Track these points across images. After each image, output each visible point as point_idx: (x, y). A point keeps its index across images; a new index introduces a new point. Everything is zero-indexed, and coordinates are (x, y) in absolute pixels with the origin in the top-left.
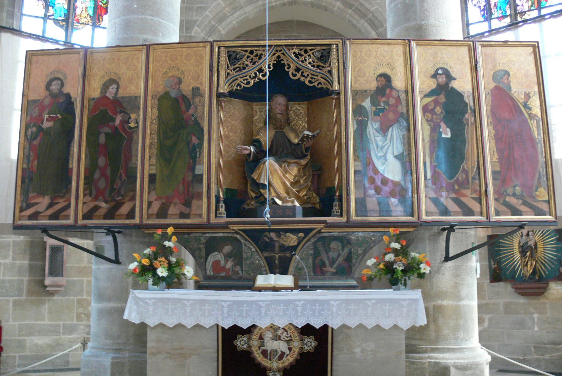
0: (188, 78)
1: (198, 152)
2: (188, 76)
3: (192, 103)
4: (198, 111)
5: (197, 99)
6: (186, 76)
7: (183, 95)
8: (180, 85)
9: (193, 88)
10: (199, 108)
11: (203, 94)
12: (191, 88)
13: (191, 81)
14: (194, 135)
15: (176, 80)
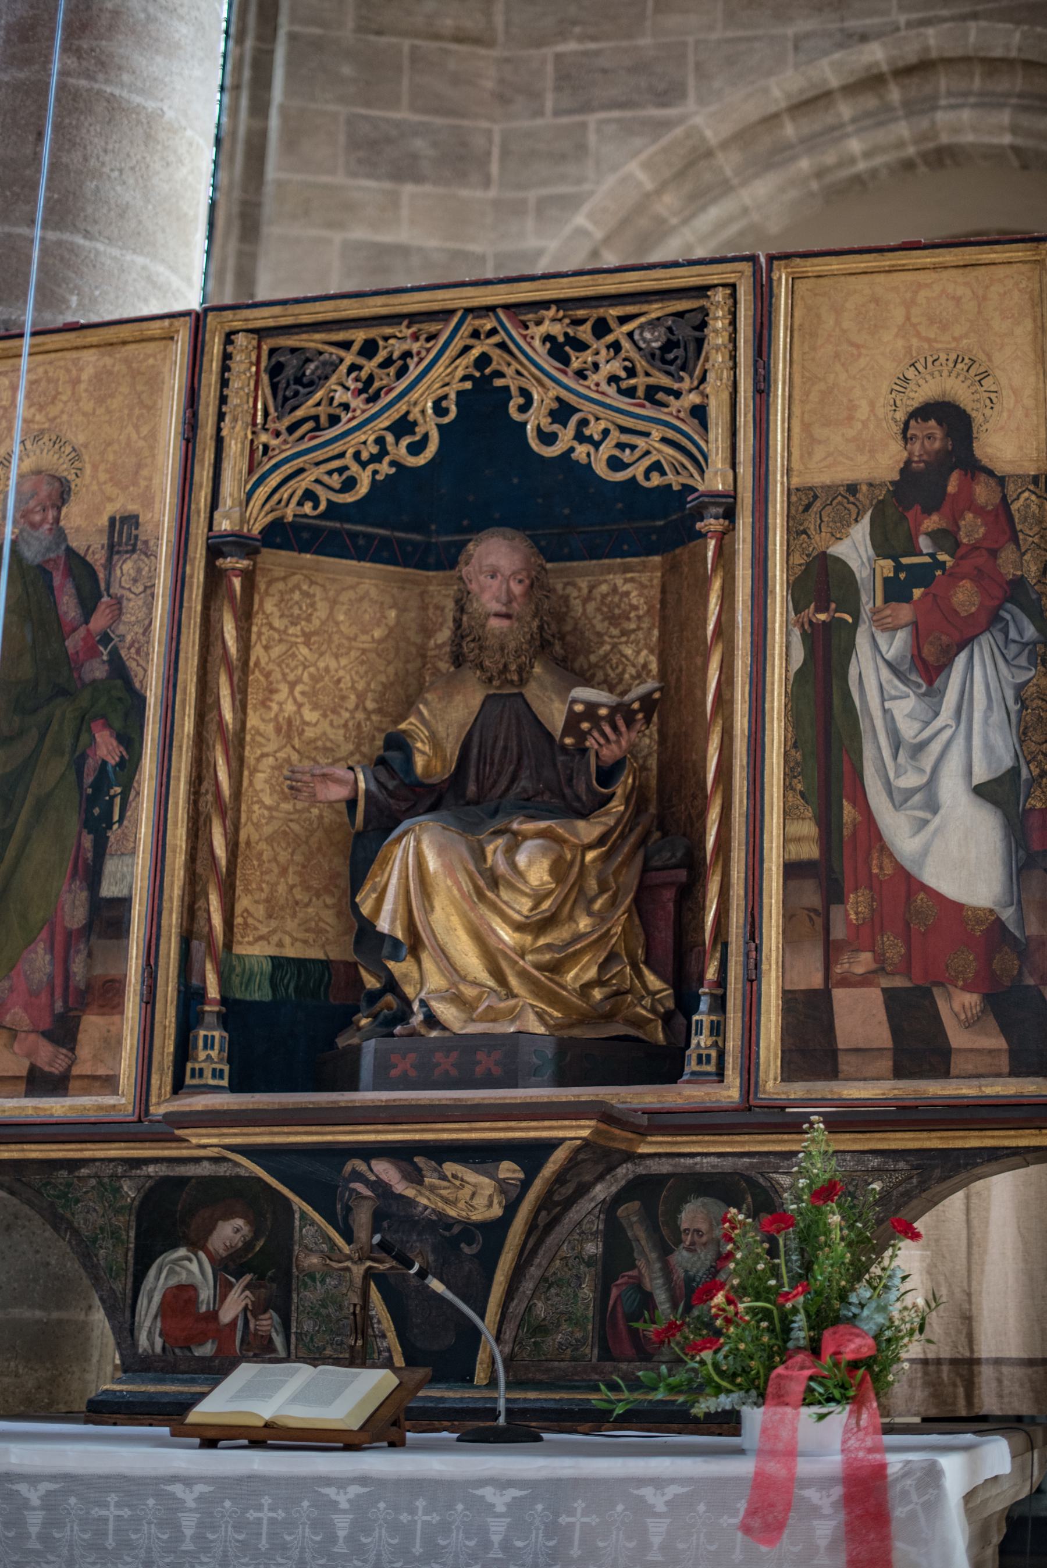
0: (94, 477)
1: (118, 801)
2: (95, 467)
3: (103, 586)
4: (123, 618)
5: (125, 567)
6: (88, 471)
7: (70, 552)
8: (59, 510)
9: (112, 520)
10: (133, 606)
11: (151, 543)
12: (104, 521)
13: (109, 489)
14: (108, 725)
15: (45, 490)
